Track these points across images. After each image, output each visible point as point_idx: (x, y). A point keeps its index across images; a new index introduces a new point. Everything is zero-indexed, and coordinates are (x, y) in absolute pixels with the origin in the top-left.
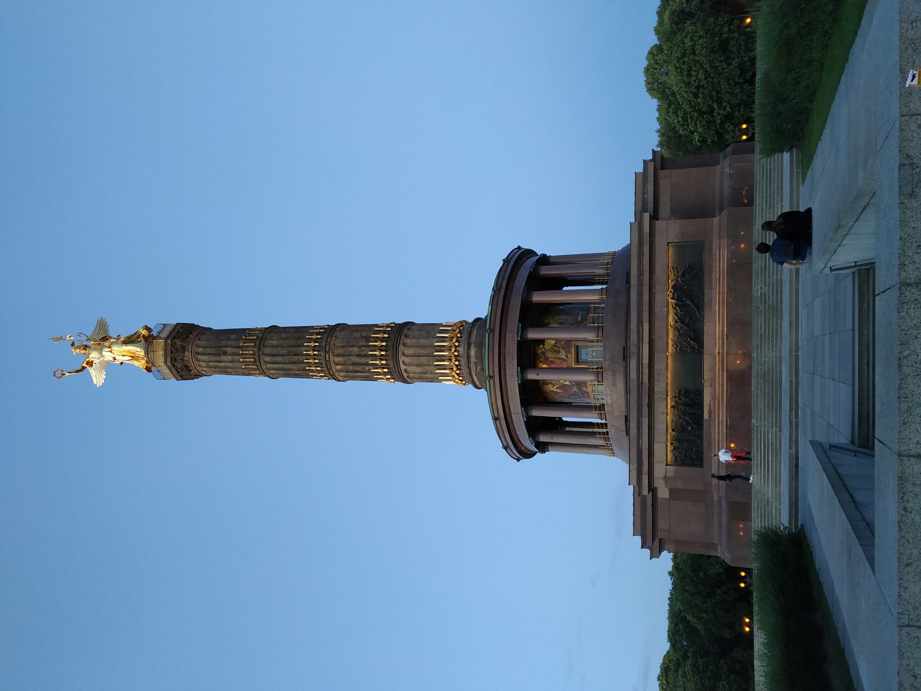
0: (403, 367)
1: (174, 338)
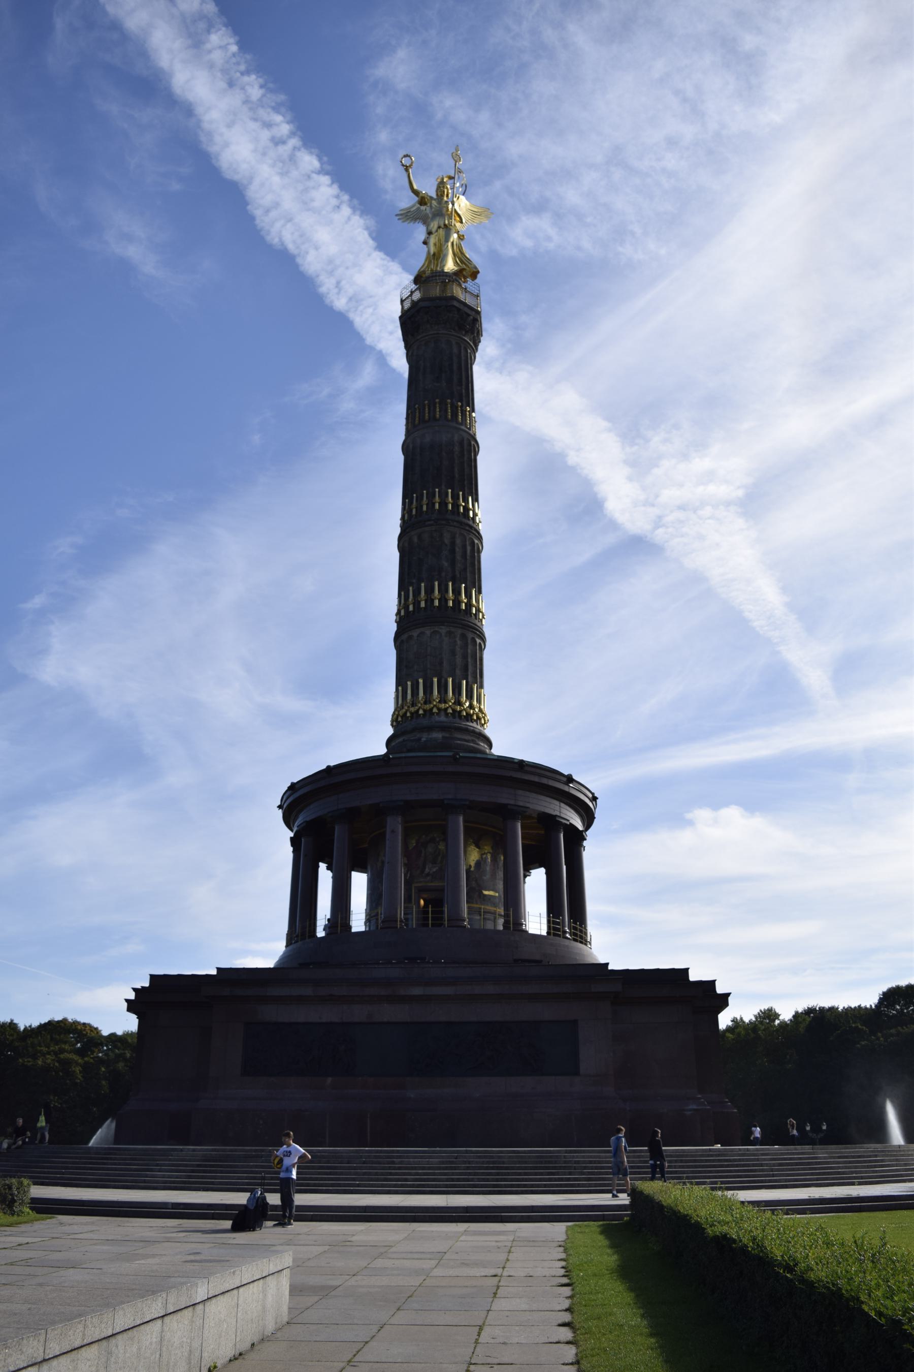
0: (415, 633)
1: (459, 310)
